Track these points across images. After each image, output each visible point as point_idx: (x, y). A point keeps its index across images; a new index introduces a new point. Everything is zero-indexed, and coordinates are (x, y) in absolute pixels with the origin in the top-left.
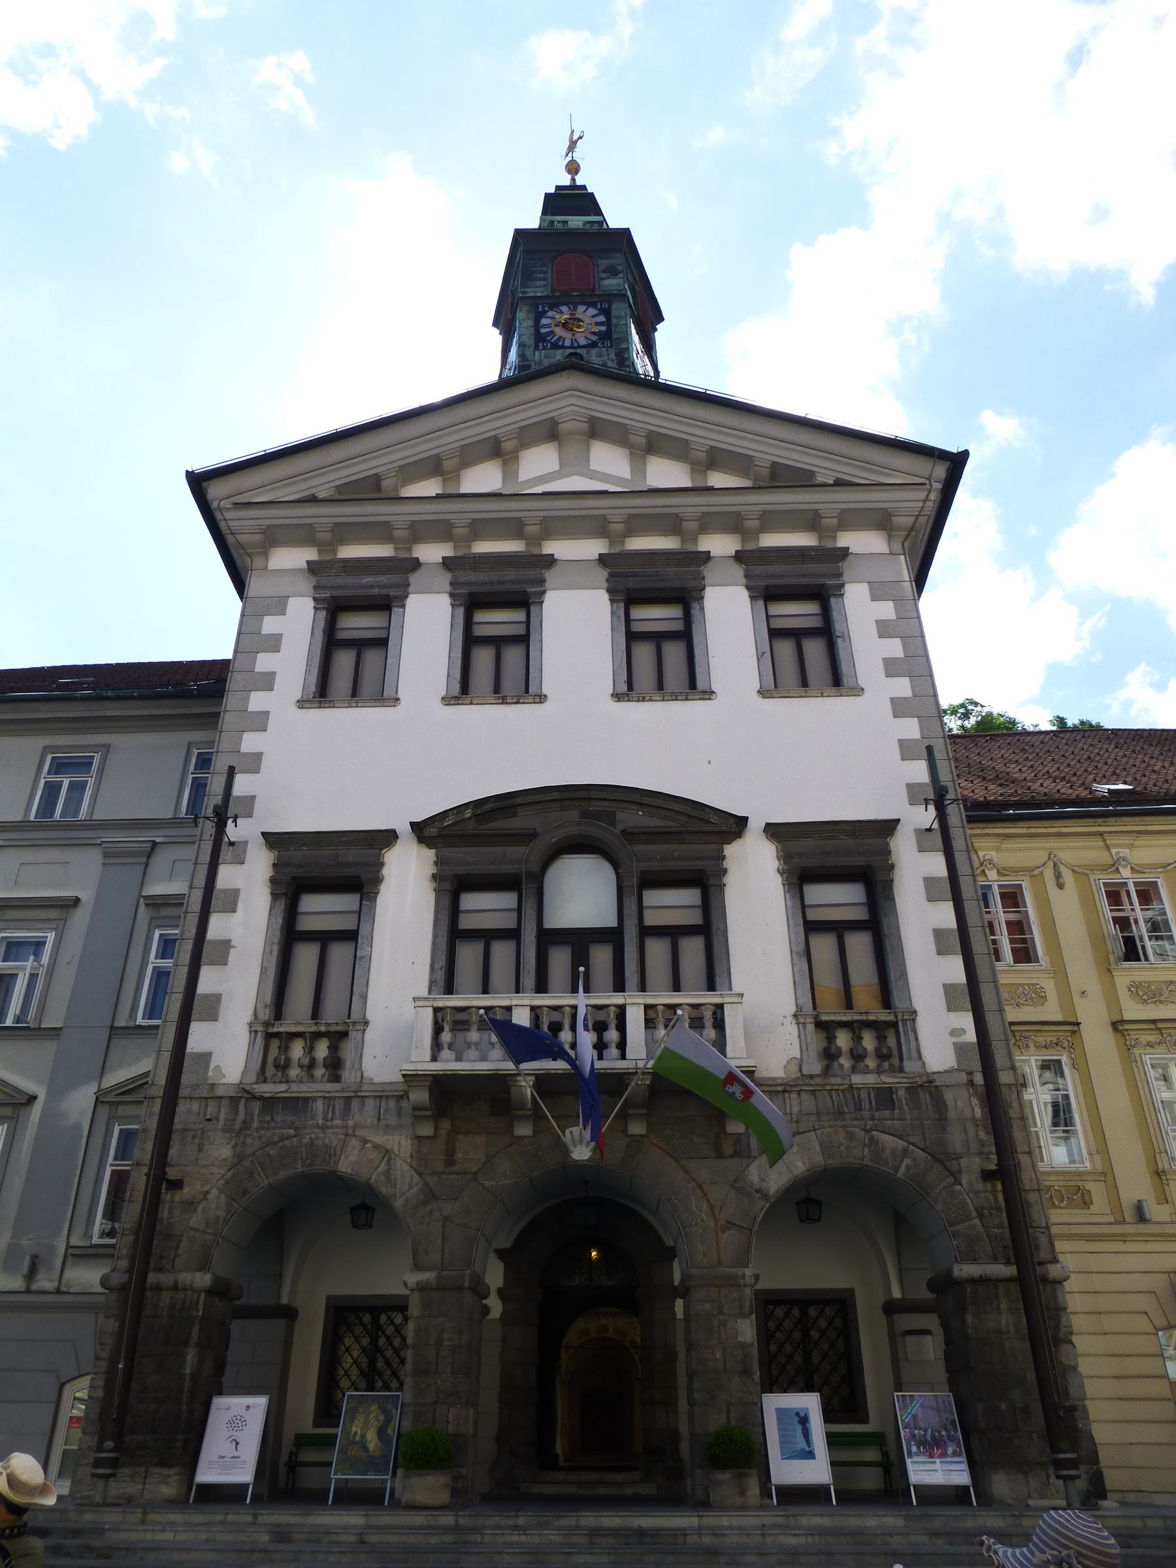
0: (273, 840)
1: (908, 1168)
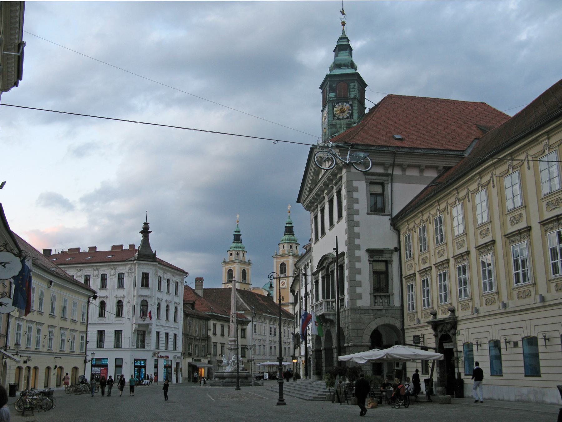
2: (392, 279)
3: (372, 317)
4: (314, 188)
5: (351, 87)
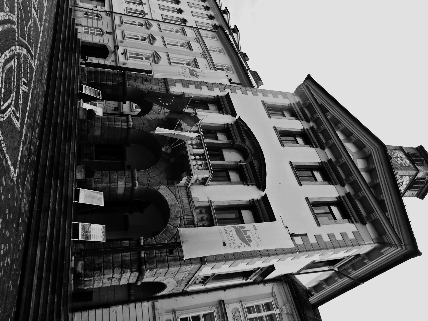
0: (228, 96)
1: (171, 227)
3: (180, 279)
4: (326, 117)
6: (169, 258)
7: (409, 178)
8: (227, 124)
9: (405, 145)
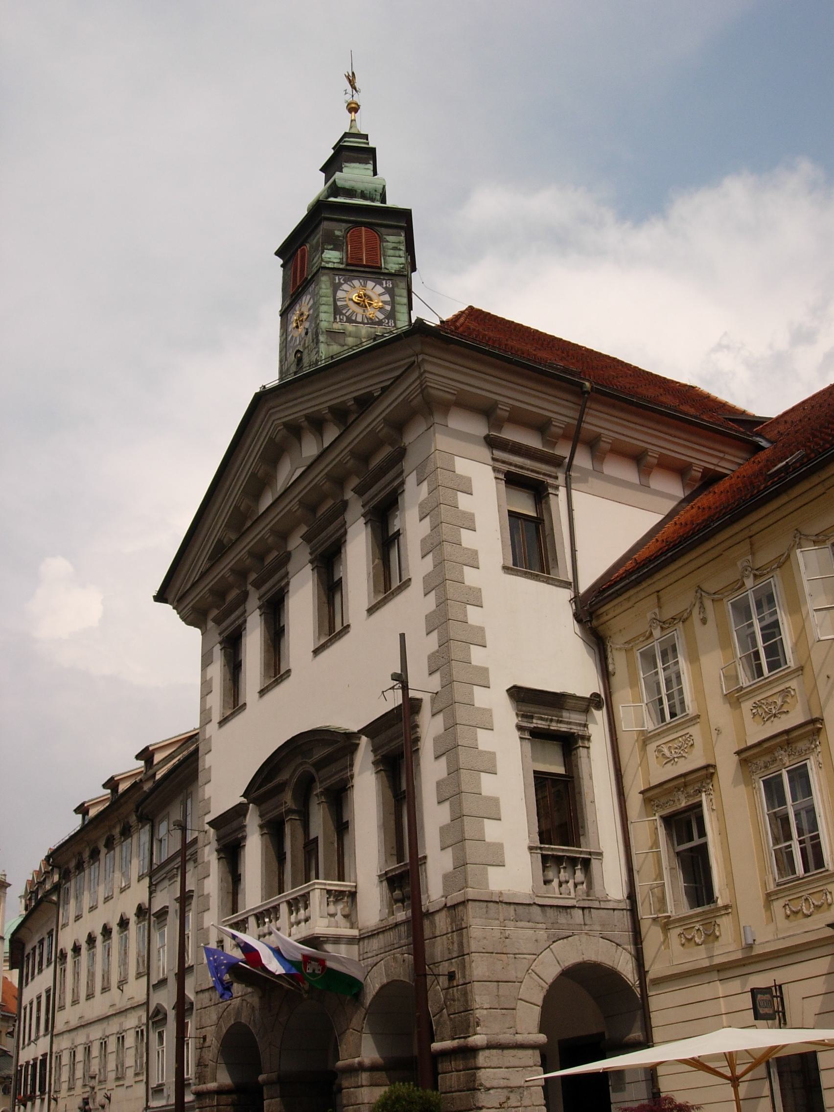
2: (593, 802)
3: (542, 934)
4: (234, 544)
5: (391, 245)
6: (461, 982)
7: (345, 287)
8: (261, 827)
9: (277, 303)
